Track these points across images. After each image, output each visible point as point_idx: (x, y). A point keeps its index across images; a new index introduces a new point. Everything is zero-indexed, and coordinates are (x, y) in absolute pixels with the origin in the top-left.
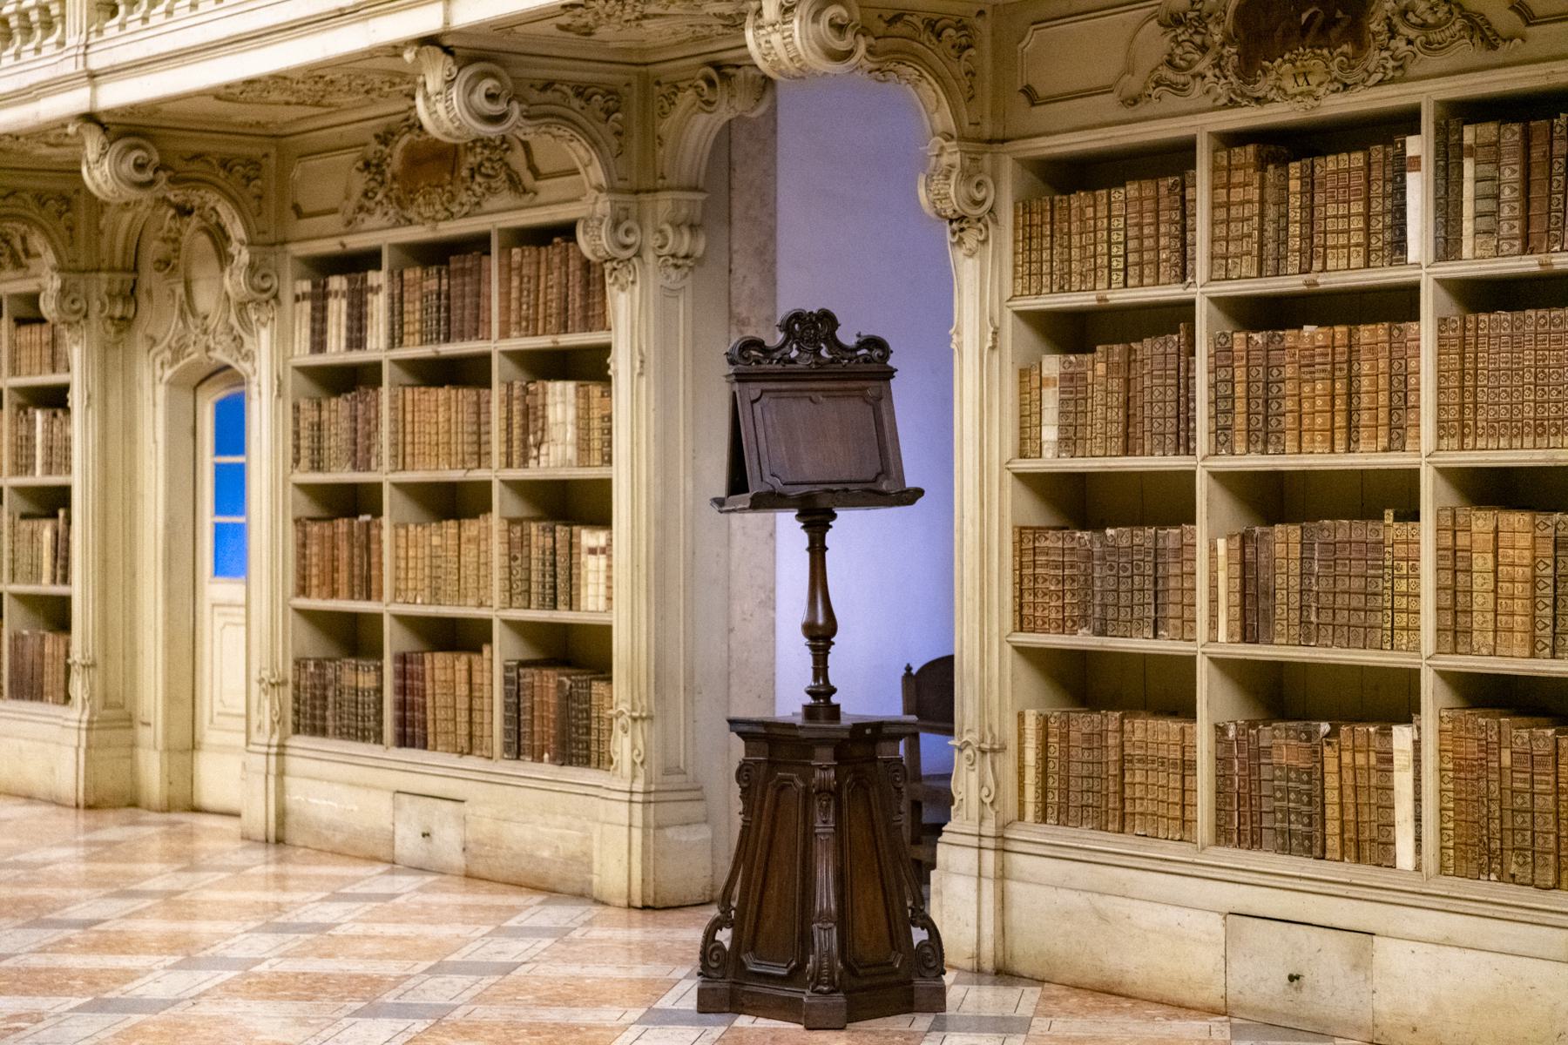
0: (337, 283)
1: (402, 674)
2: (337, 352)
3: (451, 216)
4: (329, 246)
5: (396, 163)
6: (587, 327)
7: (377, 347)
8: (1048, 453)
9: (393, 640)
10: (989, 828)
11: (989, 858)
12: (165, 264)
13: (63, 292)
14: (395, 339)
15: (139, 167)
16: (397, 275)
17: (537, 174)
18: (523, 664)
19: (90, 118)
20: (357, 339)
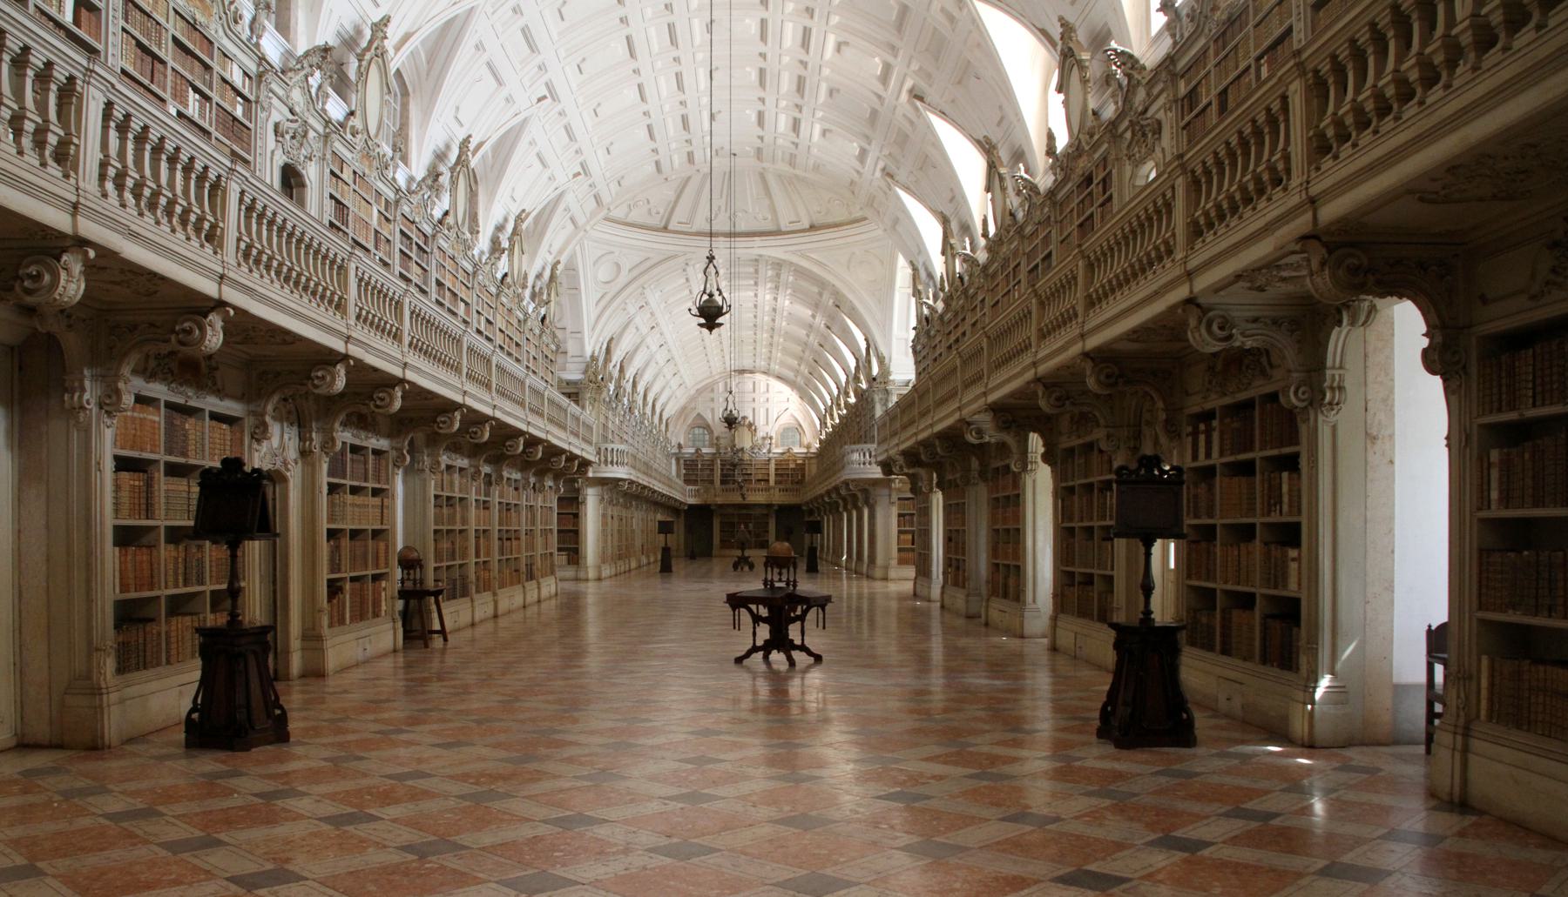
0: (1202, 427)
1: (1223, 618)
2: (1202, 461)
3: (1239, 390)
4: (1196, 409)
5: (1219, 367)
6: (1291, 444)
7: (1216, 459)
8: (1493, 507)
9: (1220, 601)
10: (1462, 721)
11: (1459, 738)
12: (1148, 423)
13: (1108, 437)
14: (1222, 454)
15: (1108, 376)
16: (1221, 421)
17: (1271, 366)
18: (1273, 616)
19: (1086, 355)
20: (1208, 455)
